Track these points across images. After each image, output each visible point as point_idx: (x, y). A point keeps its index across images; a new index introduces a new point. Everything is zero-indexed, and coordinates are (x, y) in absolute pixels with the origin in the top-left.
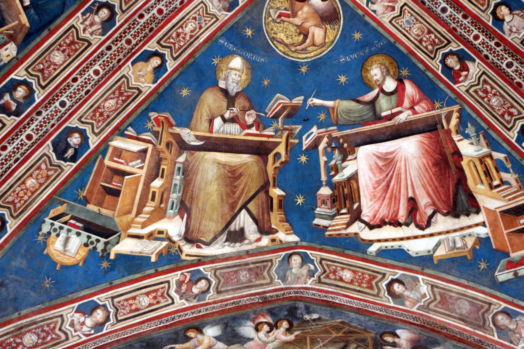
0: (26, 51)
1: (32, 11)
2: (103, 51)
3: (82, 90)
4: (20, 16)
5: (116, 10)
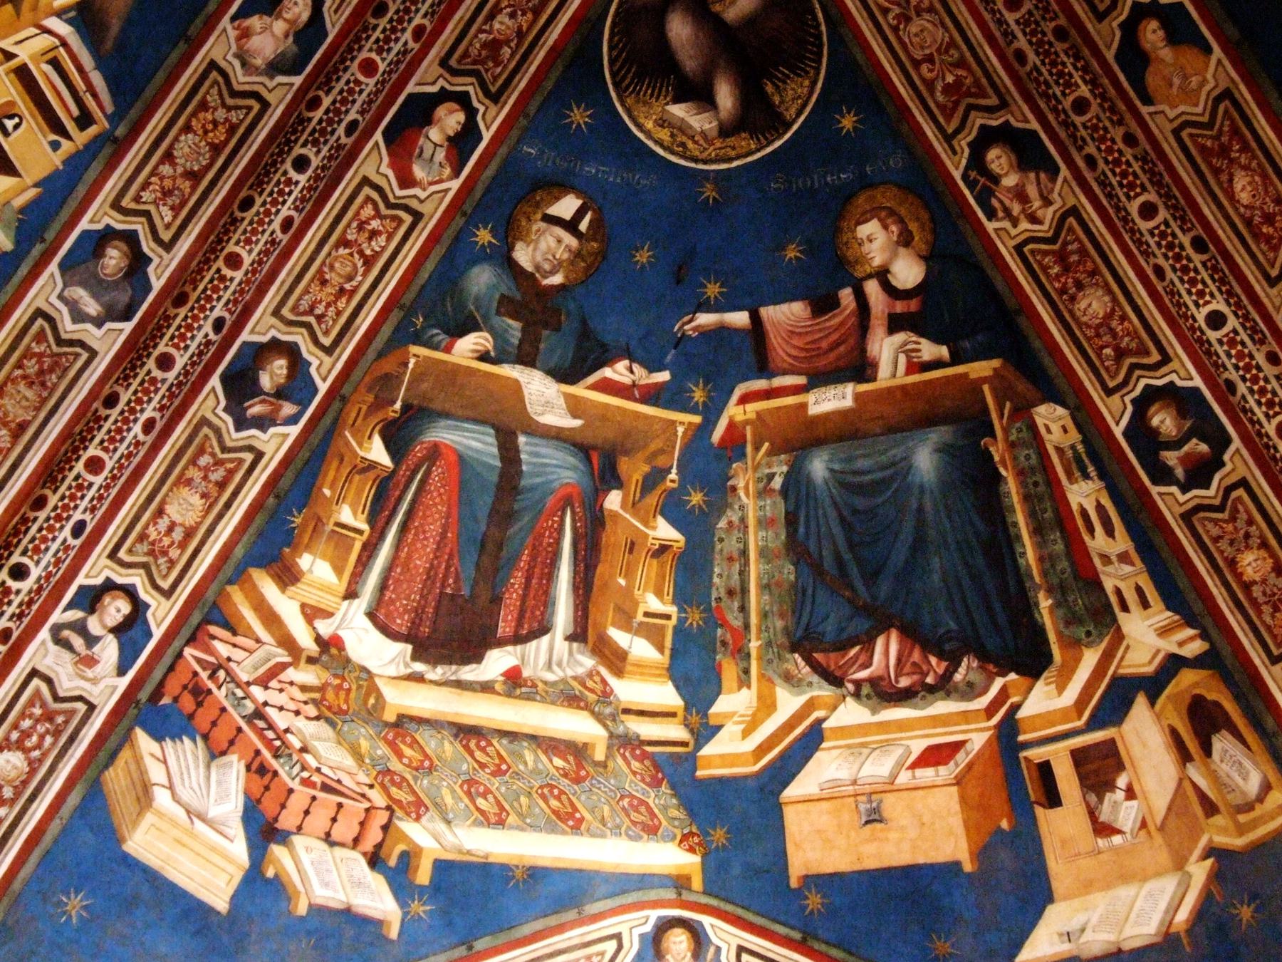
0: (1061, 382)
1: (966, 344)
2: (1096, 180)
3: (1189, 259)
4: (973, 376)
5: (995, 123)
